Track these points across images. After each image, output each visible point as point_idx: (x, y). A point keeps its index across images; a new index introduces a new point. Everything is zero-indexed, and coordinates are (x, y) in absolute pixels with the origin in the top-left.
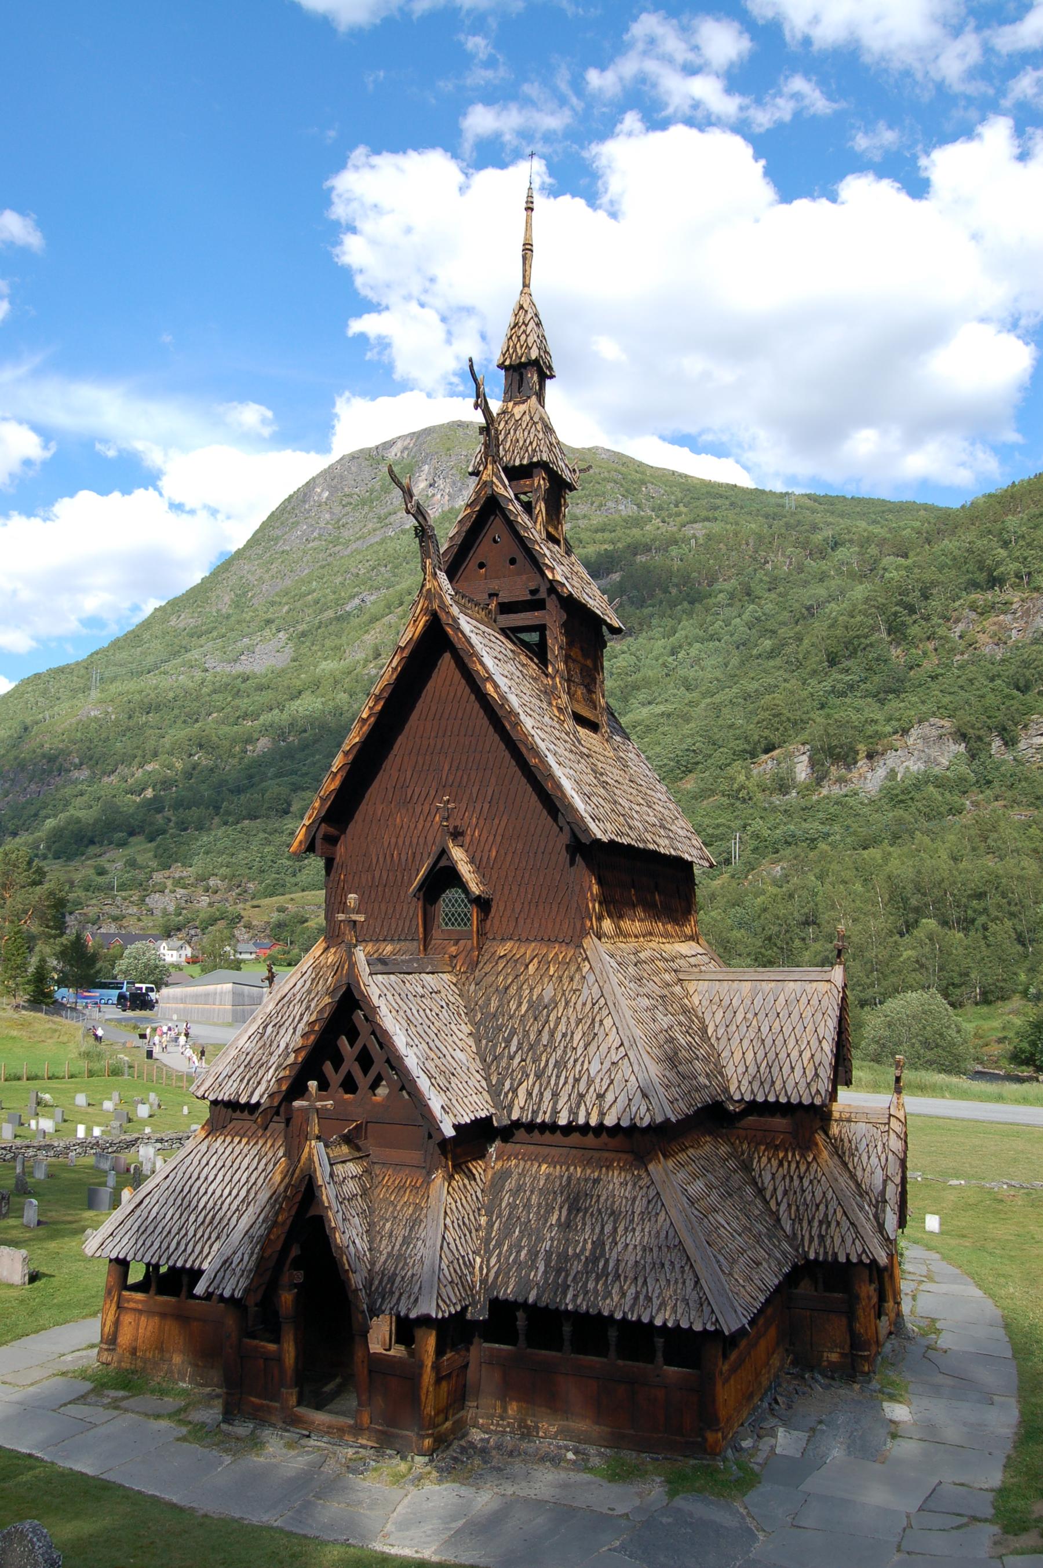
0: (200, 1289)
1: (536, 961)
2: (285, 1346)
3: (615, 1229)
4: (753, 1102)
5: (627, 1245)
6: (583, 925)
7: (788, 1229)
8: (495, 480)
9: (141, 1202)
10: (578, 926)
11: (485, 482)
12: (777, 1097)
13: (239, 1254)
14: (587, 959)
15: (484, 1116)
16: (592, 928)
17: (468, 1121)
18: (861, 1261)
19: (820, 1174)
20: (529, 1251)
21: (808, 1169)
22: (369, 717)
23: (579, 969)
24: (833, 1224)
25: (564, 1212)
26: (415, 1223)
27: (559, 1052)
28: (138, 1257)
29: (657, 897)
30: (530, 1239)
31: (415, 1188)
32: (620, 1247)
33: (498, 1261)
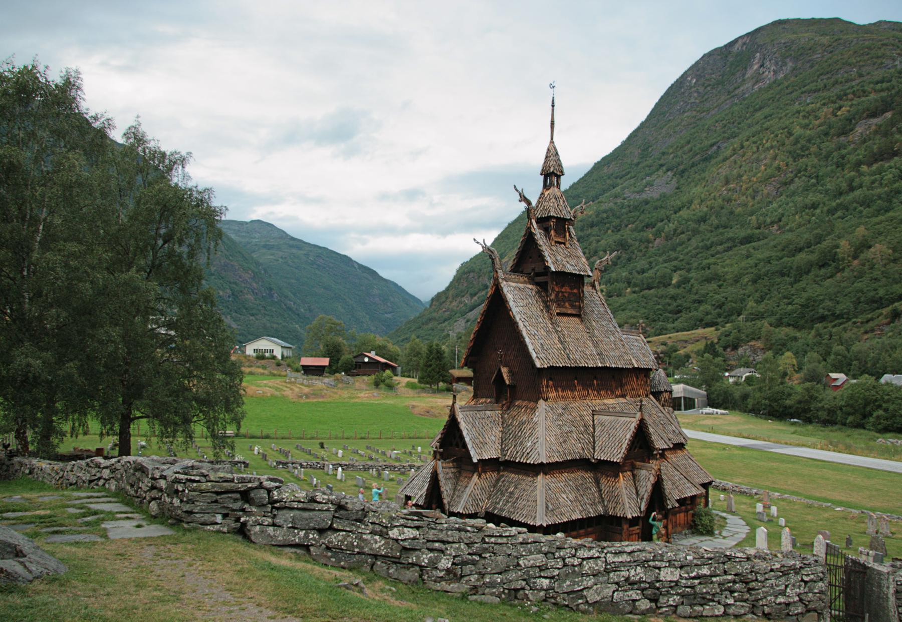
7: (606, 503)
26: (466, 487)
29: (595, 382)
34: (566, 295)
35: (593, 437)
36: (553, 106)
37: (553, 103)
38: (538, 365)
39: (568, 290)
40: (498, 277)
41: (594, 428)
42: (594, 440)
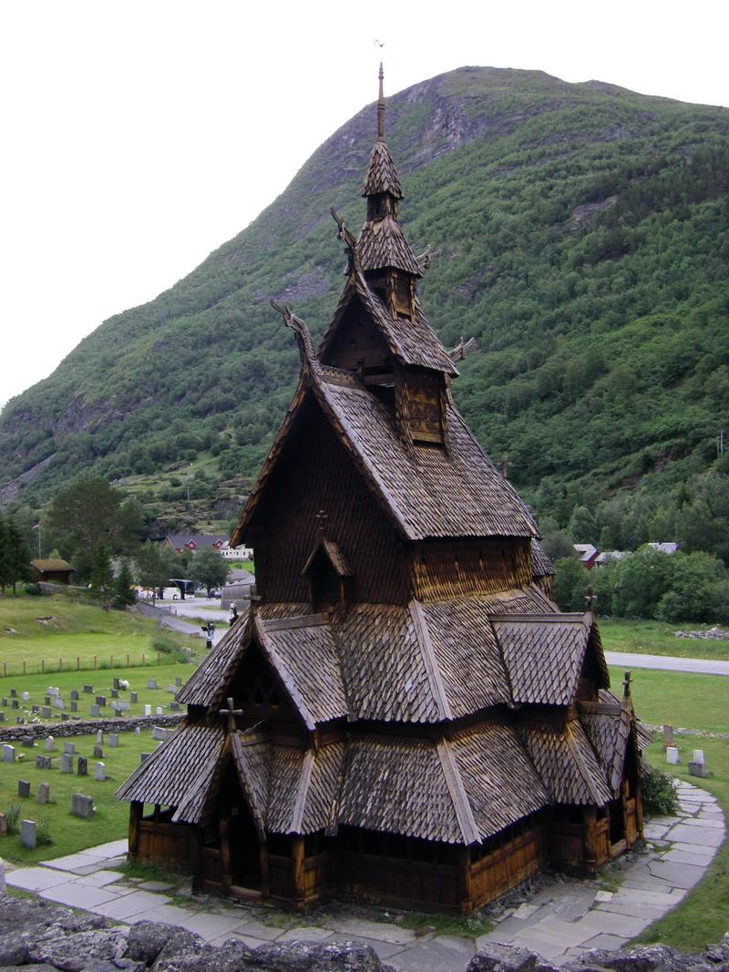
0: (175, 818)
1: (380, 616)
2: (224, 851)
3: (414, 784)
4: (527, 703)
5: (419, 794)
6: (409, 592)
7: (546, 783)
8: (358, 284)
9: (148, 767)
10: (406, 594)
11: (351, 286)
12: (541, 700)
13: (197, 798)
14: (410, 616)
15: (340, 716)
16: (415, 595)
17: (328, 720)
18: (588, 804)
19: (567, 749)
20: (364, 797)
21: (560, 745)
22: (273, 458)
23: (405, 623)
24: (574, 780)
25: (387, 774)
26: (295, 779)
27: (388, 676)
28: (165, 803)
29: (481, 564)
30: (365, 789)
31: (295, 761)
32: (415, 795)
33: (346, 803)
34: (422, 408)
35: (503, 662)
36: (381, 78)
37: (381, 73)
38: (412, 534)
39: (425, 401)
40: (312, 372)
41: (500, 648)
42: (505, 666)
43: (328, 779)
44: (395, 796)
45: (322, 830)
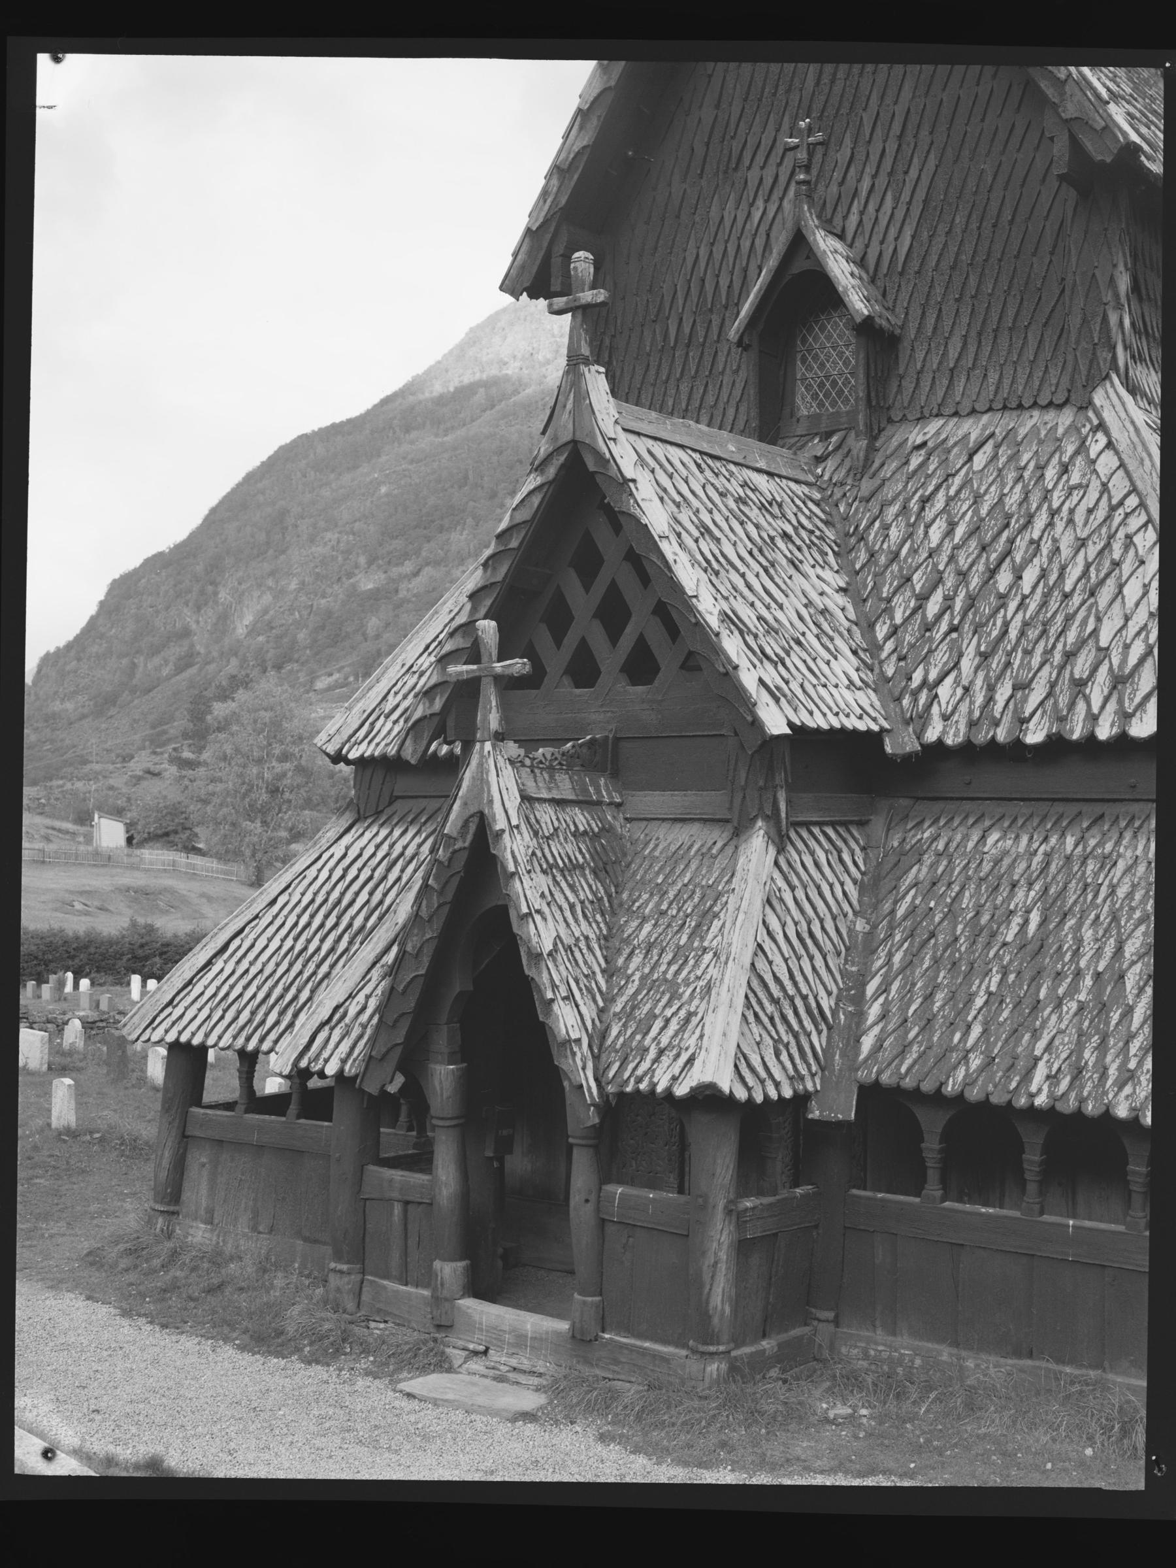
13: (361, 997)
14: (1102, 426)
16: (1115, 368)
23: (1082, 448)
25: (1035, 918)
33: (883, 1016)
43: (816, 929)
44: (1073, 989)
45: (802, 1100)
